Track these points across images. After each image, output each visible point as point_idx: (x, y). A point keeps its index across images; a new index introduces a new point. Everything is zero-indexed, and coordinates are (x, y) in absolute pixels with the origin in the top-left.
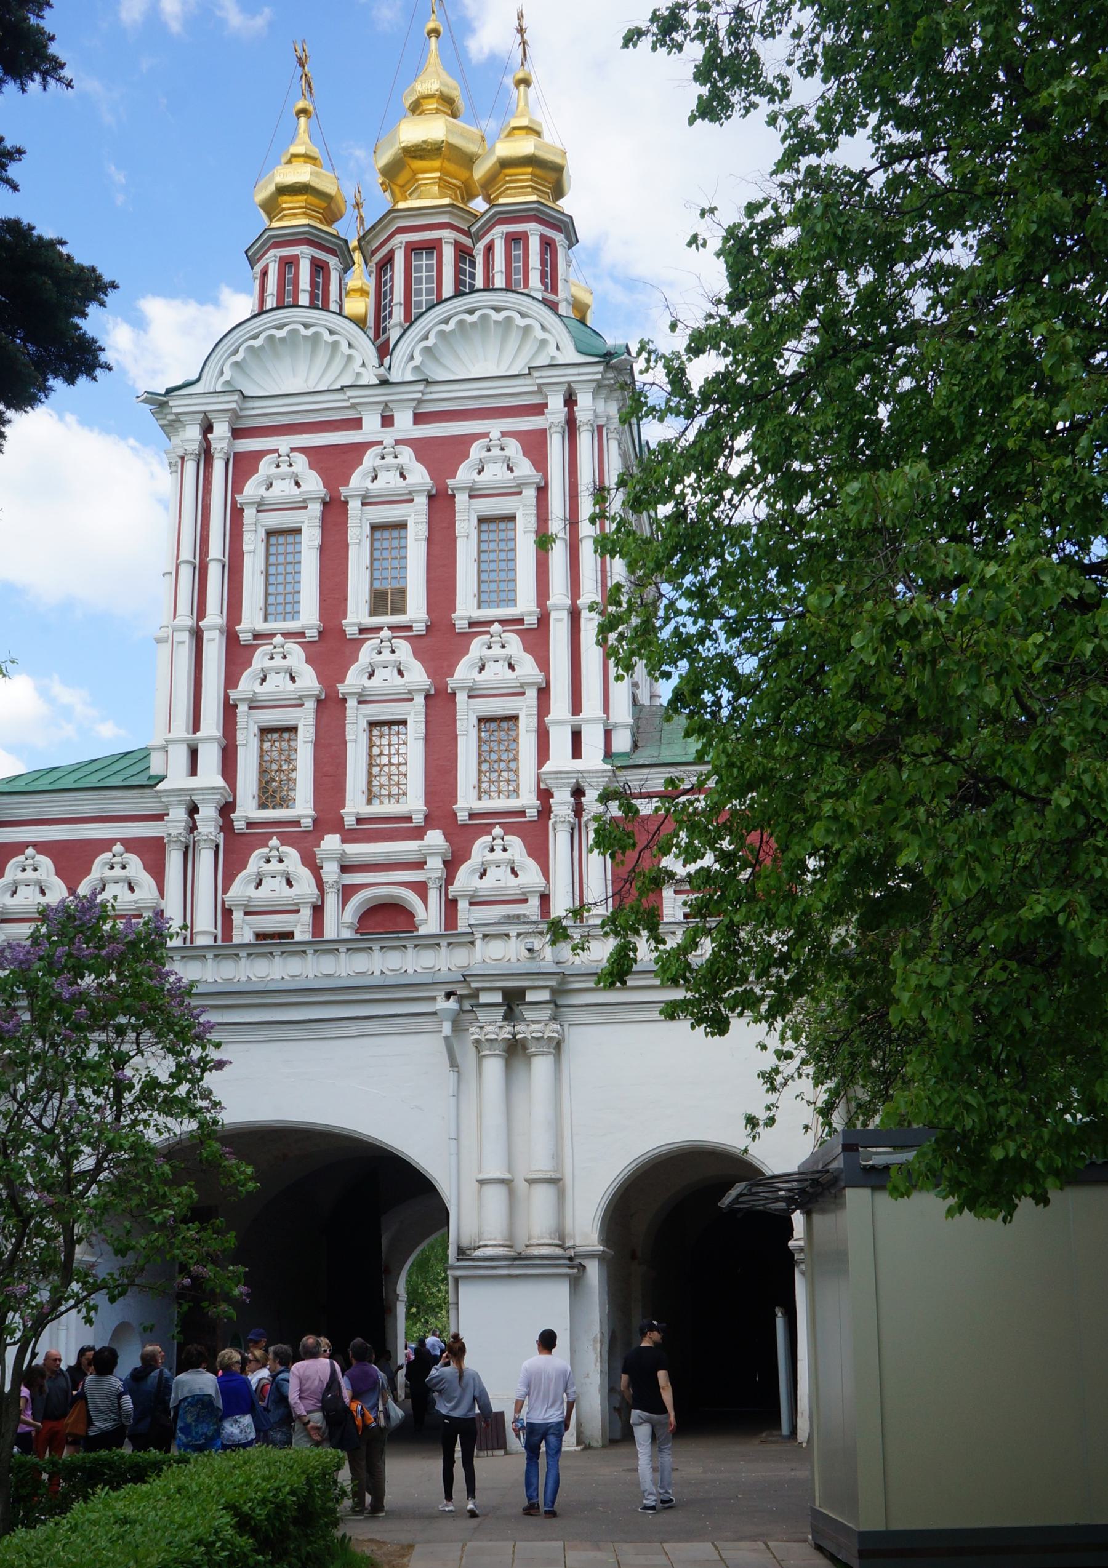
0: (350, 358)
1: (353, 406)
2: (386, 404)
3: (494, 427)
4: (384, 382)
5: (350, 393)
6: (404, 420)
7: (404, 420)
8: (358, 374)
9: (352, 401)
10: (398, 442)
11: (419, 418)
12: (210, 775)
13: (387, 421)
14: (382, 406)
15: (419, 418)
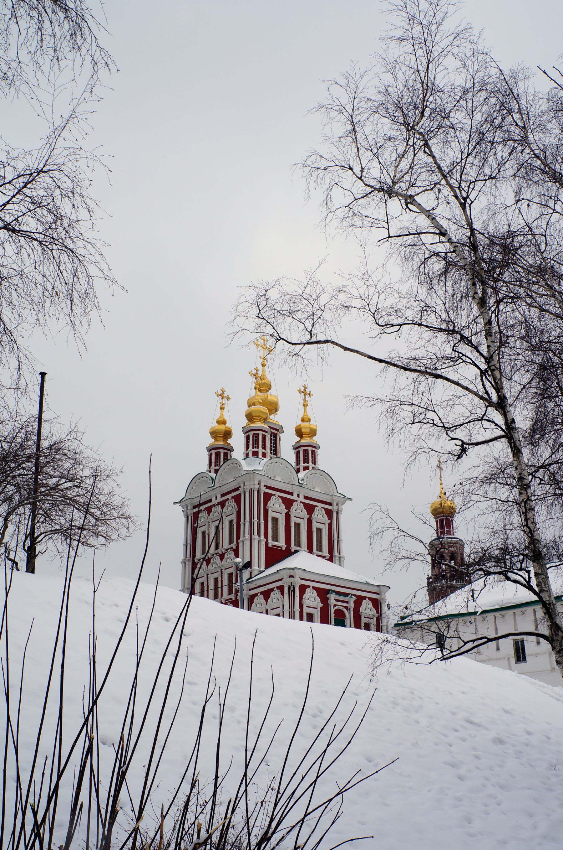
3: (320, 505)
13: (298, 496)
15: (306, 498)
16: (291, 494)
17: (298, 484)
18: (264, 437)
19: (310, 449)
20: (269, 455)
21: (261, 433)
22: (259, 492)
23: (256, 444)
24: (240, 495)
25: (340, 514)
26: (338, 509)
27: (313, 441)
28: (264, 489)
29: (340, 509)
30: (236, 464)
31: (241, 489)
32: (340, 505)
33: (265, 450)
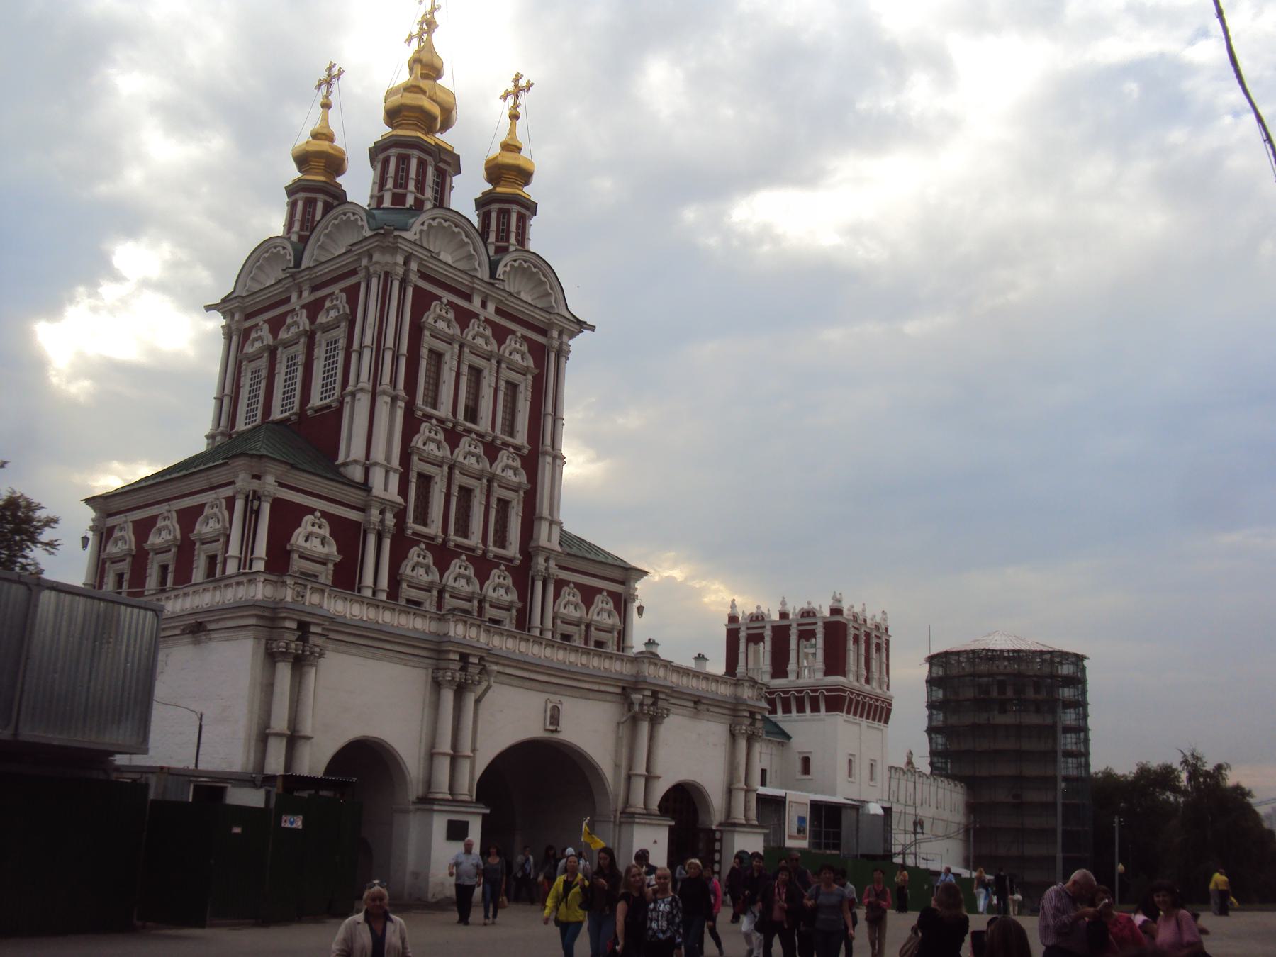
0: (472, 255)
1: (473, 288)
2: (487, 294)
4: (492, 284)
5: (476, 281)
6: (491, 307)
7: (491, 307)
8: (476, 270)
9: (475, 286)
10: (487, 321)
11: (498, 311)
12: (393, 494)
13: (484, 305)
14: (484, 295)
16: (468, 298)
17: (487, 278)
18: (422, 164)
19: (515, 209)
20: (428, 205)
21: (415, 152)
22: (404, 282)
23: (402, 172)
24: (358, 285)
25: (563, 359)
26: (561, 344)
27: (521, 193)
28: (414, 278)
29: (564, 347)
30: (354, 214)
31: (362, 274)
32: (565, 338)
33: (423, 193)
